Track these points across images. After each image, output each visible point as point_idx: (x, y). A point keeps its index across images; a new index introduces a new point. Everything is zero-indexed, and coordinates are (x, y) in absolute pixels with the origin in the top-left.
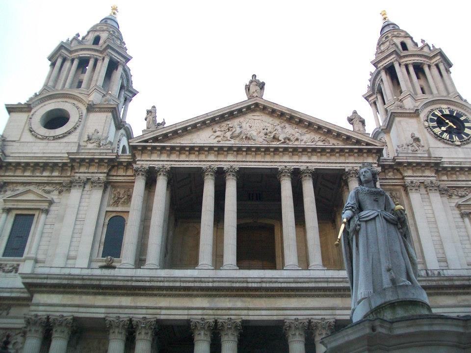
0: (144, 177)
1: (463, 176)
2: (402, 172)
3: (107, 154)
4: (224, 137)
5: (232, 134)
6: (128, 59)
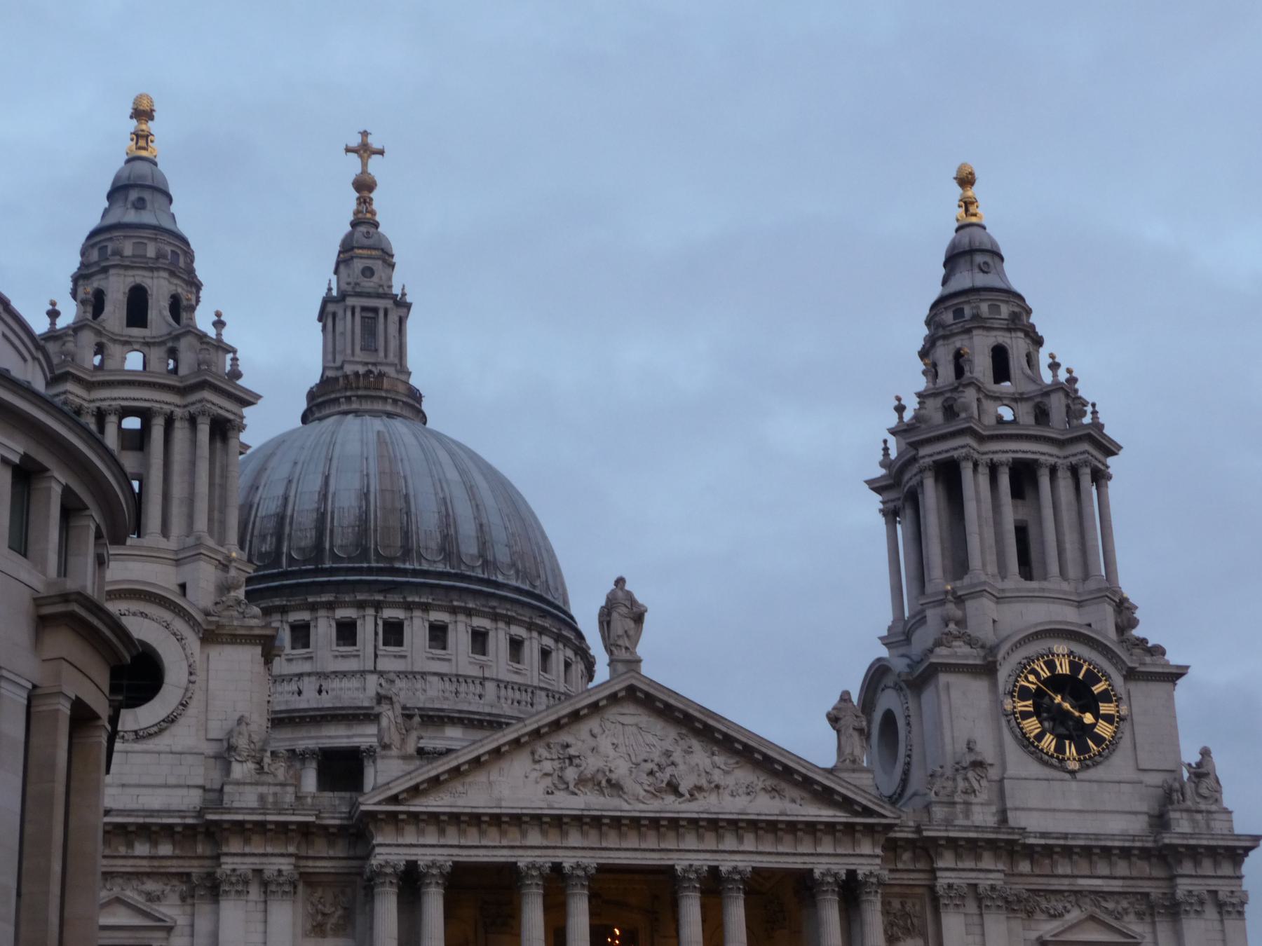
0: (395, 890)
1: (1067, 860)
2: (933, 856)
3: (296, 812)
4: (560, 777)
5: (579, 776)
6: (246, 399)
